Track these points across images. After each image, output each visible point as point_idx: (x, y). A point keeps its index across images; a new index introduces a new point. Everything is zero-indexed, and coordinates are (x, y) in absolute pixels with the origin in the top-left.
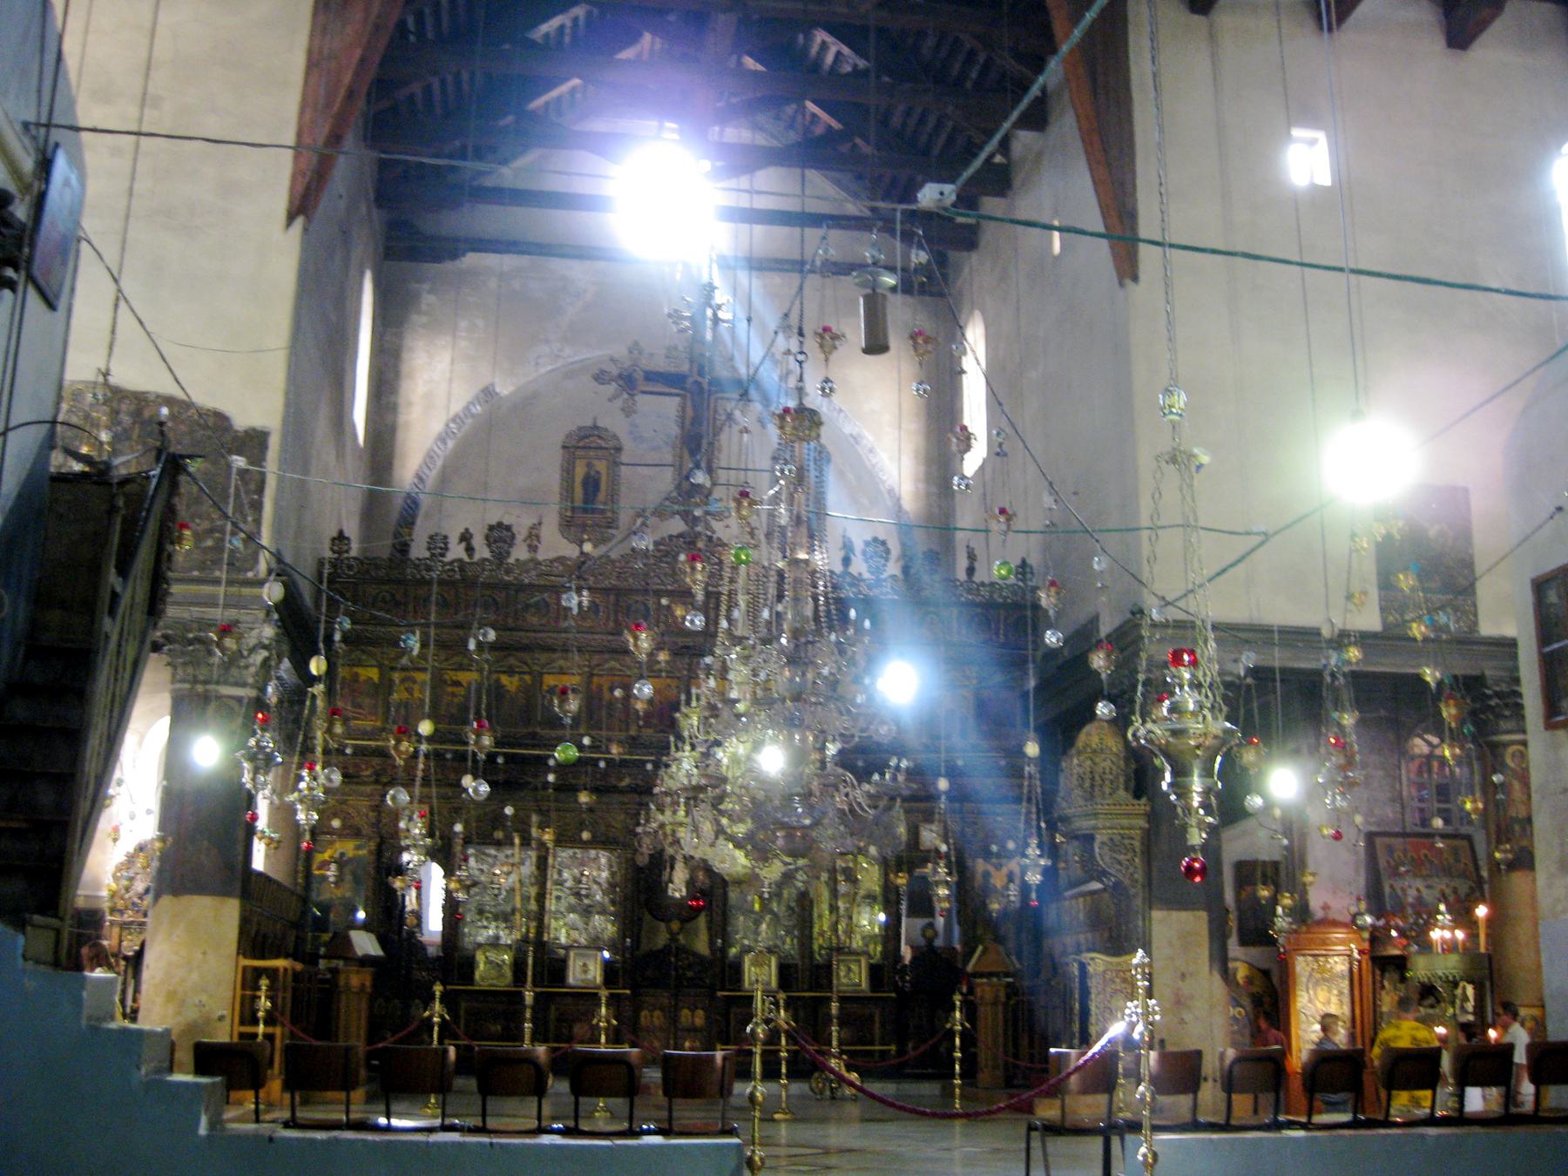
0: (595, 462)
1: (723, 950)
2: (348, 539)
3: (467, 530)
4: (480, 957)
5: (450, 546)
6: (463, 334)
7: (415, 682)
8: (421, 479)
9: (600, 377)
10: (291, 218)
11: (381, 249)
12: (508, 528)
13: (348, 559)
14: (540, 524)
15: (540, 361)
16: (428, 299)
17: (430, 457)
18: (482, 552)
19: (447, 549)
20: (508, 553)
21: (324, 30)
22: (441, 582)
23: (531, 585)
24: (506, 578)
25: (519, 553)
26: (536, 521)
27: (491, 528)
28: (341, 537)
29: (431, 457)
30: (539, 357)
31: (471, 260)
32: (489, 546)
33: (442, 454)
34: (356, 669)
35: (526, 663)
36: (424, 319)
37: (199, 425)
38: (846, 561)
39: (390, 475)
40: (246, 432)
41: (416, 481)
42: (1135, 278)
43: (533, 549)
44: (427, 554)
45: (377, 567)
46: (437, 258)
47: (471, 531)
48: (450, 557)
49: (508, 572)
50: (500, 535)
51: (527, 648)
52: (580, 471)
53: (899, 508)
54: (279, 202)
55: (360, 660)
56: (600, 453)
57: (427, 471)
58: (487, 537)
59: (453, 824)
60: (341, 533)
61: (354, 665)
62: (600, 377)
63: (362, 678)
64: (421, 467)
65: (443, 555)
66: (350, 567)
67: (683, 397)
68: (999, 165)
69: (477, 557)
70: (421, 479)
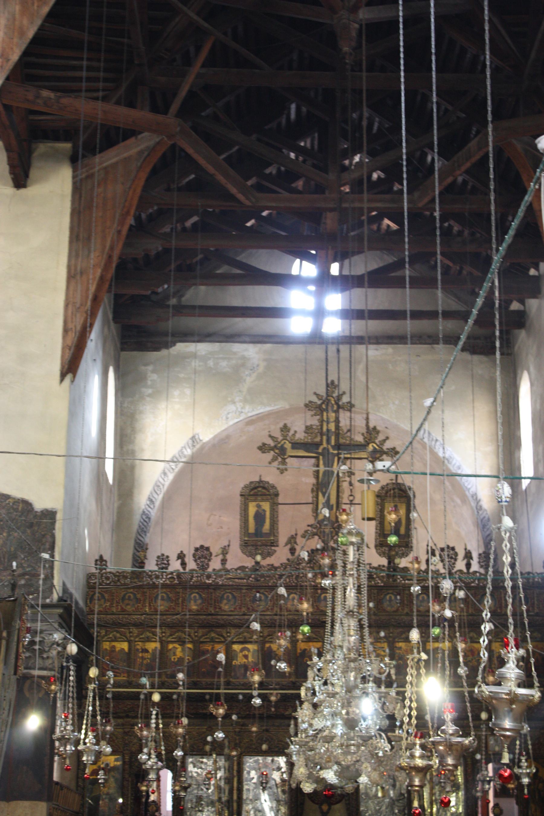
2: (106, 561)
3: (182, 552)
5: (170, 562)
6: (177, 400)
8: (151, 501)
9: (263, 448)
10: (63, 376)
11: (119, 345)
12: (208, 549)
13: (106, 573)
14: (229, 546)
15: (229, 416)
16: (153, 377)
17: (157, 486)
18: (191, 565)
19: (169, 564)
20: (208, 565)
21: (77, 256)
22: (164, 586)
23: (223, 585)
24: (207, 581)
25: (215, 564)
26: (226, 544)
27: (197, 549)
28: (101, 560)
29: (158, 486)
30: (228, 413)
31: (181, 347)
32: (195, 561)
34: (113, 644)
35: (222, 636)
36: (150, 391)
37: (14, 509)
39: (132, 499)
40: (42, 512)
41: (148, 503)
43: (224, 561)
44: (156, 568)
45: (125, 577)
47: (185, 552)
48: (171, 569)
49: (209, 577)
51: (223, 626)
52: (252, 509)
53: (479, 508)
54: (56, 367)
56: (264, 497)
57: (156, 496)
58: (194, 555)
60: (101, 557)
61: (113, 641)
62: (263, 448)
63: (117, 649)
64: (151, 493)
65: (167, 568)
66: (107, 578)
67: (317, 458)
68: (534, 276)
69: (187, 570)
70: (151, 501)
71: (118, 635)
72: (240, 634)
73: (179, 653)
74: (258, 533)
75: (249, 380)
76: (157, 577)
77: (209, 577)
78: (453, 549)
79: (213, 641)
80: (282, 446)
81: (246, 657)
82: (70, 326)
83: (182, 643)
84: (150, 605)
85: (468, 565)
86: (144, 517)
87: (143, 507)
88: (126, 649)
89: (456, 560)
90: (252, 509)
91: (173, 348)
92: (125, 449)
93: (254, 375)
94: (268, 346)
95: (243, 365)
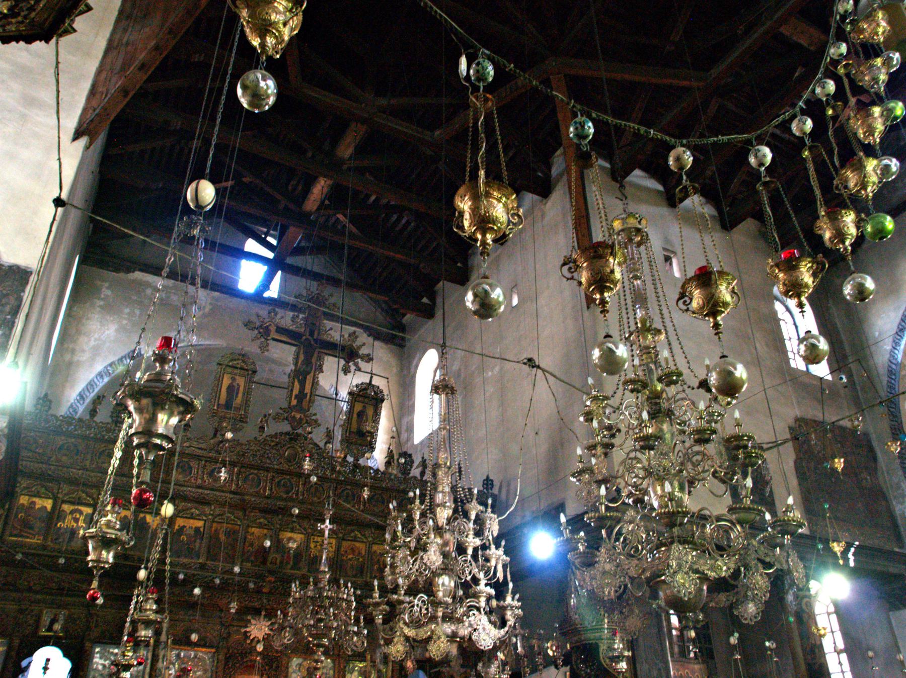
0: (237, 377)
7: (81, 513)
29: (92, 385)
31: (138, 275)
34: (34, 499)
36: (102, 303)
46: (117, 270)
52: (226, 382)
55: (38, 492)
56: (242, 372)
57: (88, 394)
59: (202, 594)
61: (35, 496)
63: (37, 507)
64: (83, 390)
71: (43, 490)
72: (187, 509)
74: (228, 405)
78: (410, 456)
80: (267, 327)
84: (92, 460)
85: (423, 473)
86: (71, 410)
87: (72, 401)
88: (49, 507)
89: (411, 467)
90: (226, 382)
91: (131, 274)
92: (66, 346)
94: (216, 294)
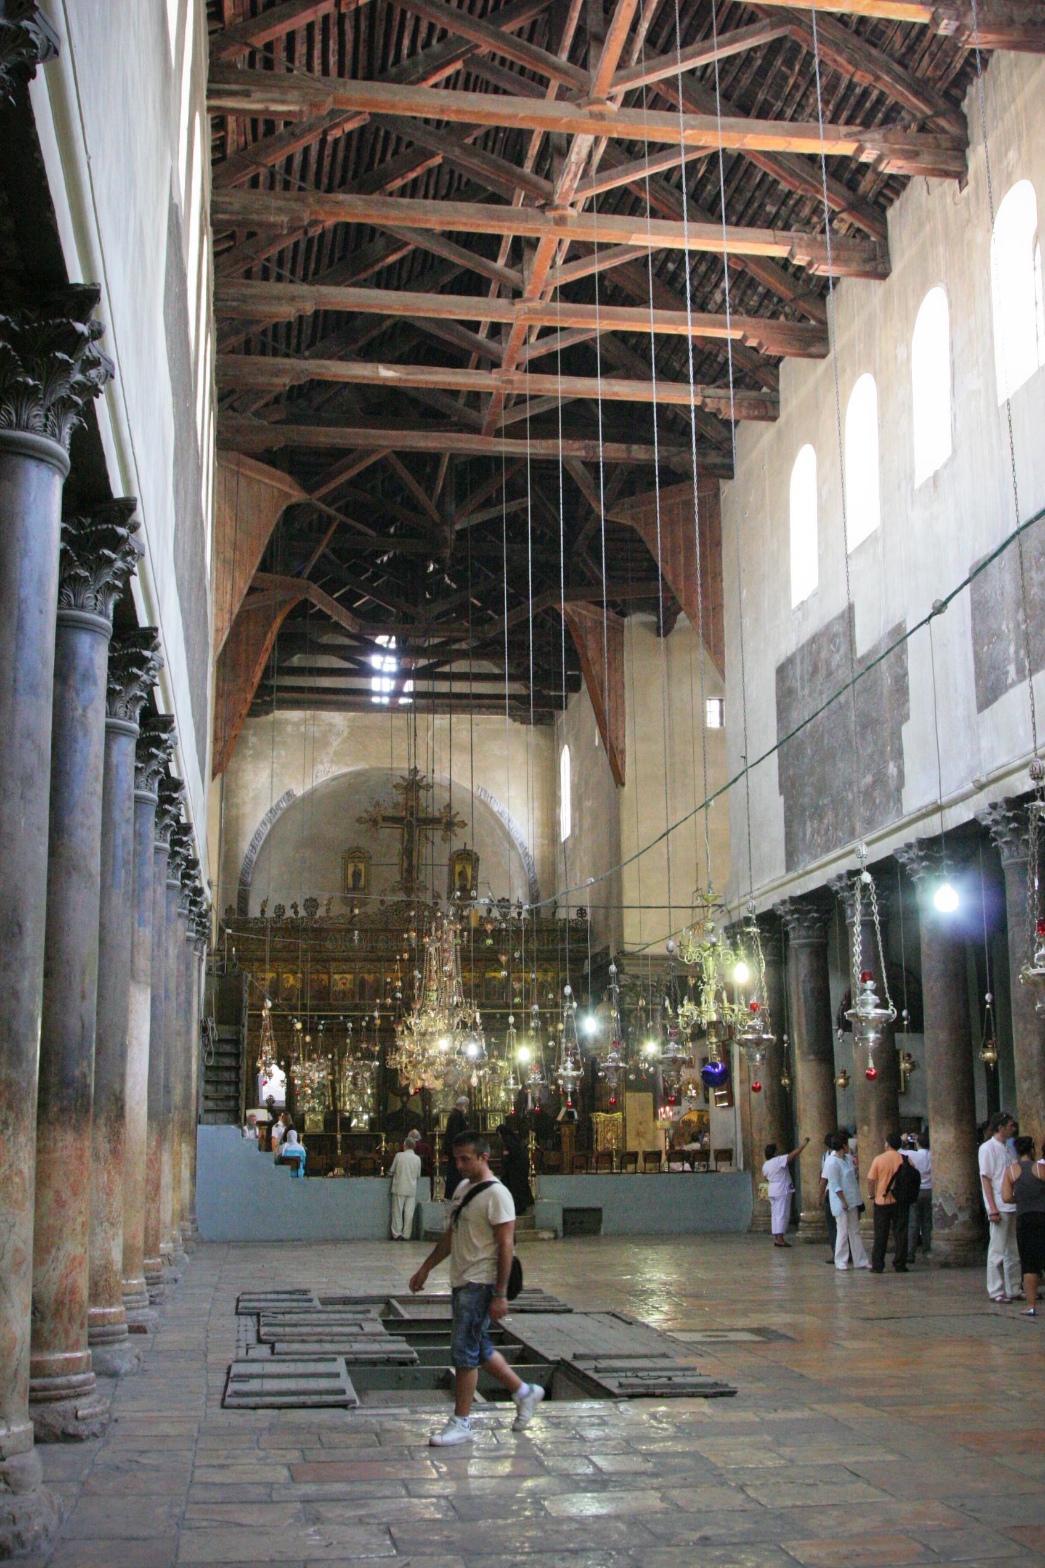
1: (430, 1111)
4: (307, 1118)
9: (359, 820)
16: (253, 740)
17: (258, 834)
18: (302, 913)
21: (224, 680)
25: (321, 912)
27: (307, 900)
31: (278, 714)
33: (266, 831)
36: (251, 752)
38: (489, 911)
42: (623, 784)
49: (316, 922)
50: (312, 904)
73: (292, 981)
74: (355, 888)
75: (335, 744)
76: (275, 922)
77: (316, 922)
79: (318, 972)
81: (344, 984)
82: (220, 735)
83: (295, 973)
93: (340, 740)
95: (330, 731)
